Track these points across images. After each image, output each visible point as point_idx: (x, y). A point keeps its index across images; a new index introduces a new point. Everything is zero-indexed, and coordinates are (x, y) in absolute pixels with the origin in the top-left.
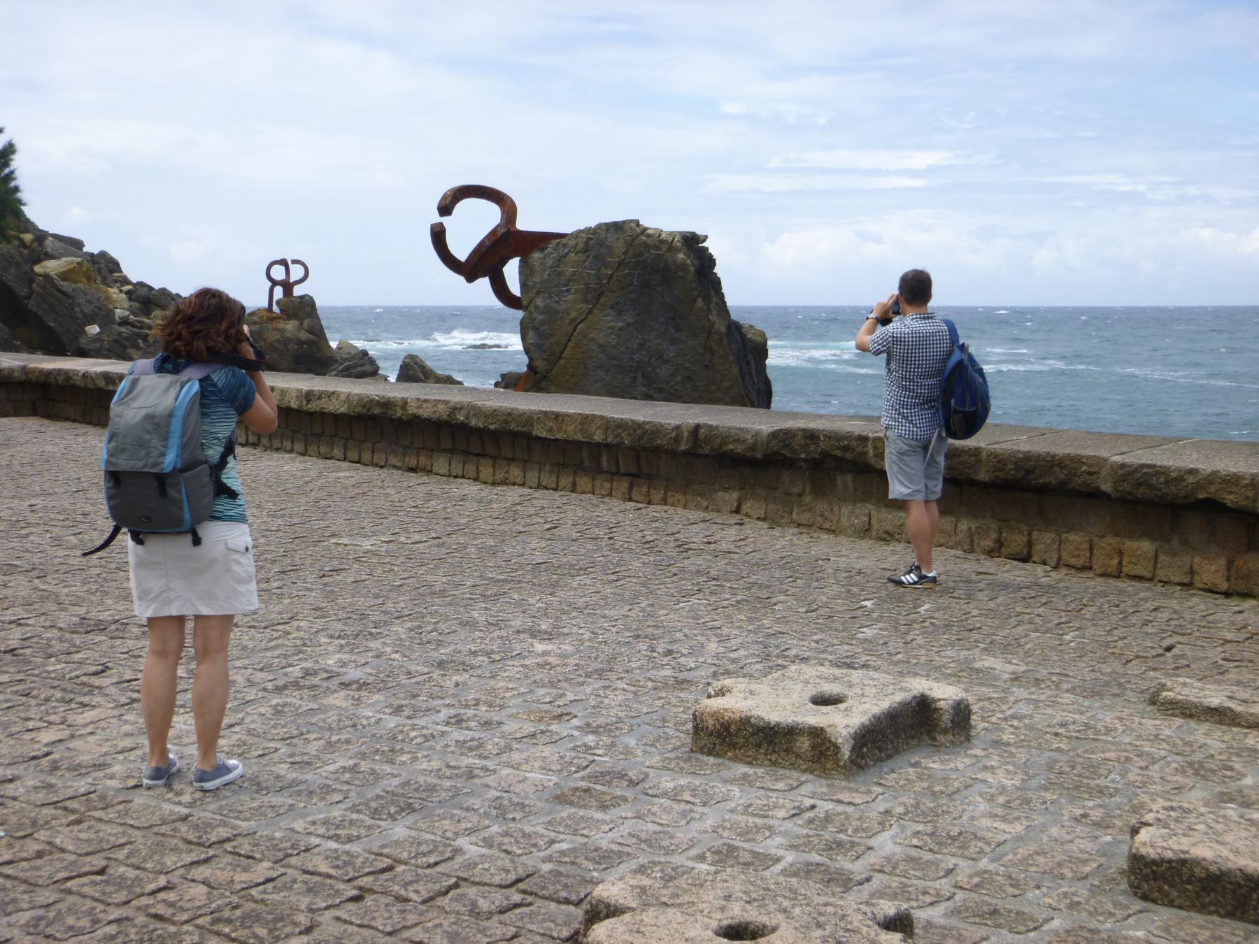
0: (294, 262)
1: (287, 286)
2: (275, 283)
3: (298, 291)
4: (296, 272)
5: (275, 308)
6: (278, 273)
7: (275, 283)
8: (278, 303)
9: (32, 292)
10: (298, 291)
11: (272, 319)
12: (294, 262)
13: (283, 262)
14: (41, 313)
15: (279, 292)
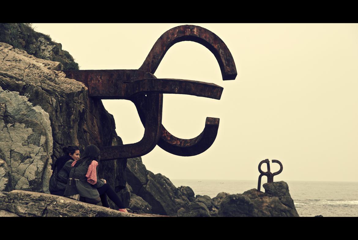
0: (274, 161)
1: (270, 176)
2: (262, 174)
3: (276, 179)
4: (275, 168)
5: (263, 190)
6: (264, 168)
7: (262, 174)
8: (264, 186)
9: (147, 180)
10: (276, 179)
11: (262, 195)
12: (274, 161)
13: (267, 161)
14: (153, 193)
15: (265, 179)
